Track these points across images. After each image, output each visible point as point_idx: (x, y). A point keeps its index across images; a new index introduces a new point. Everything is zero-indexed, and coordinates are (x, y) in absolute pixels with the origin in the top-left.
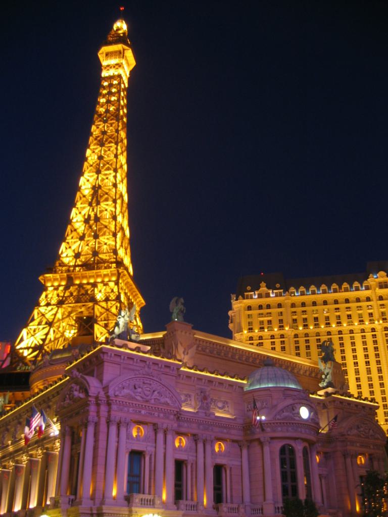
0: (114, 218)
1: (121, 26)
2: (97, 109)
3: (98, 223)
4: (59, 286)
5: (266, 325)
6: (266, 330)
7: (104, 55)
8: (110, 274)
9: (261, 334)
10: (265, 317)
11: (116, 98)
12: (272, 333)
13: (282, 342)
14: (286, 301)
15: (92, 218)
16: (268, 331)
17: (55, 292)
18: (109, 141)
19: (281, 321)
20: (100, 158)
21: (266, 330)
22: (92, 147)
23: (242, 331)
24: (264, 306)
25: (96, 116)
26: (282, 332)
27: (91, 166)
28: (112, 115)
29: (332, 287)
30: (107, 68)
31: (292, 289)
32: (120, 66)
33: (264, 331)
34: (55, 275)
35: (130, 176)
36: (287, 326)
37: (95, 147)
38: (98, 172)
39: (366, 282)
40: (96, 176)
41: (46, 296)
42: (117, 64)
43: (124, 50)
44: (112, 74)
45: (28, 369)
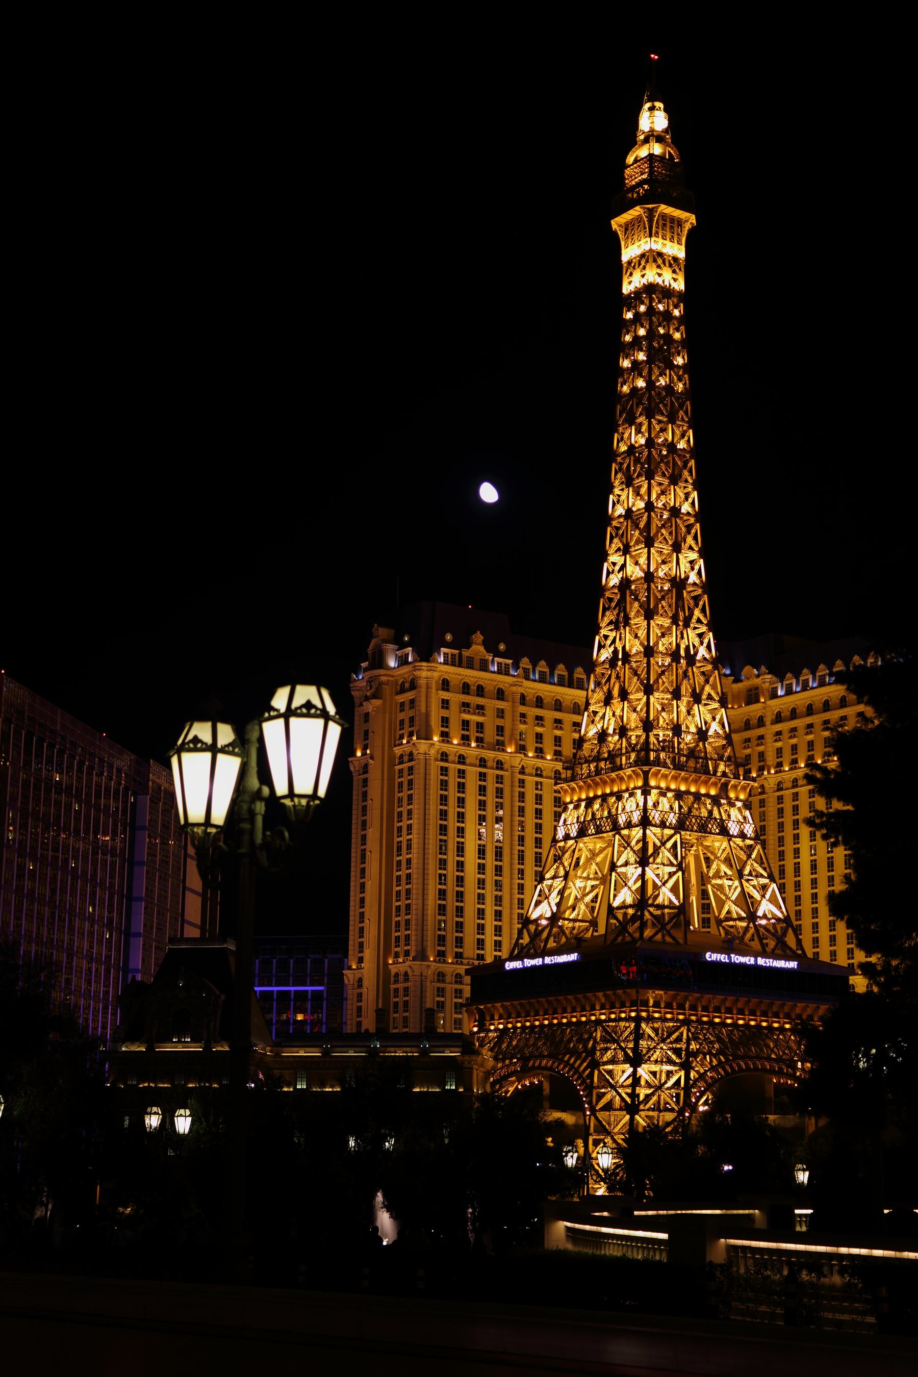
4: (668, 789)
5: (473, 733)
6: (473, 744)
9: (463, 750)
10: (474, 714)
15: (682, 653)
16: (478, 746)
23: (432, 739)
24: (473, 688)
30: (660, 261)
31: (525, 662)
33: (469, 745)
36: (510, 745)
42: (675, 259)
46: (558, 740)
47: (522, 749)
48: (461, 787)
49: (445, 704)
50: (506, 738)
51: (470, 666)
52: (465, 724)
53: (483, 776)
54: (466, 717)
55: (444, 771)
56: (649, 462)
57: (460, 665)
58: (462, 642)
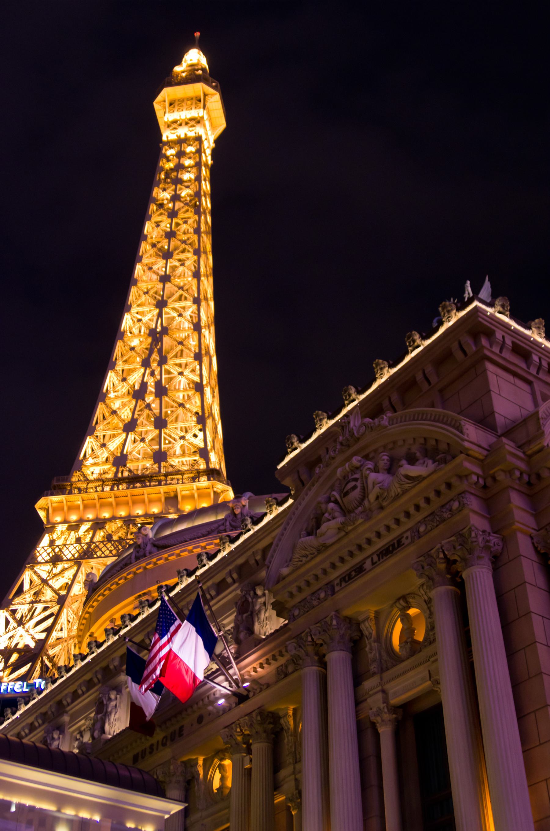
0: (199, 388)
1: (195, 57)
2: (154, 194)
3: (165, 399)
7: (167, 104)
8: (196, 496)
11: (192, 176)
15: (151, 389)
17: (73, 535)
18: (181, 249)
20: (165, 279)
22: (145, 260)
25: (153, 207)
27: (146, 293)
28: (187, 204)
32: (199, 122)
34: (71, 497)
35: (221, 321)
37: (152, 260)
38: (161, 304)
40: (157, 311)
41: (52, 543)
42: (192, 119)
43: (205, 95)
44: (183, 136)
45: (13, 690)
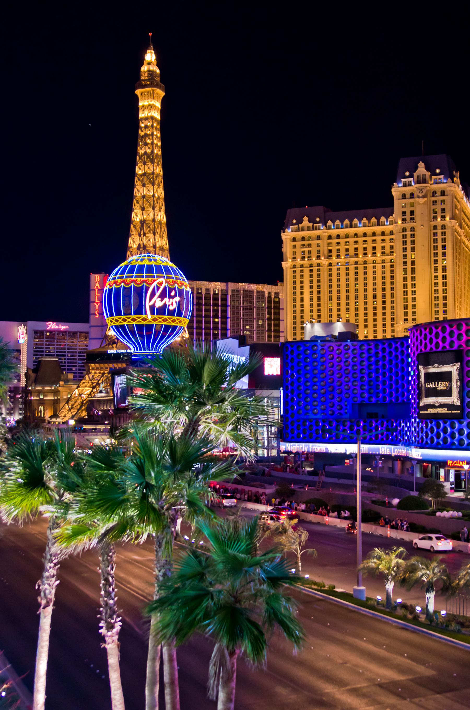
5: (306, 255)
6: (306, 259)
9: (302, 262)
12: (310, 262)
13: (319, 270)
14: (324, 234)
15: (142, 246)
19: (319, 252)
21: (306, 259)
26: (318, 261)
29: (362, 222)
30: (143, 109)
31: (330, 223)
38: (143, 209)
39: (391, 217)
42: (149, 105)
43: (153, 90)
46: (347, 250)
47: (330, 257)
48: (302, 276)
49: (294, 246)
50: (321, 254)
51: (303, 229)
52: (303, 252)
53: (311, 271)
54: (303, 249)
55: (294, 272)
56: (149, 178)
57: (299, 231)
58: (300, 221)
